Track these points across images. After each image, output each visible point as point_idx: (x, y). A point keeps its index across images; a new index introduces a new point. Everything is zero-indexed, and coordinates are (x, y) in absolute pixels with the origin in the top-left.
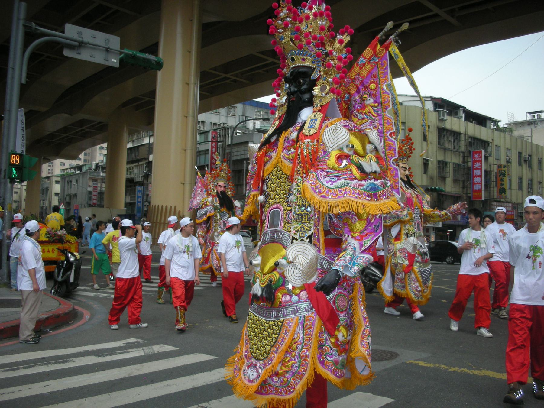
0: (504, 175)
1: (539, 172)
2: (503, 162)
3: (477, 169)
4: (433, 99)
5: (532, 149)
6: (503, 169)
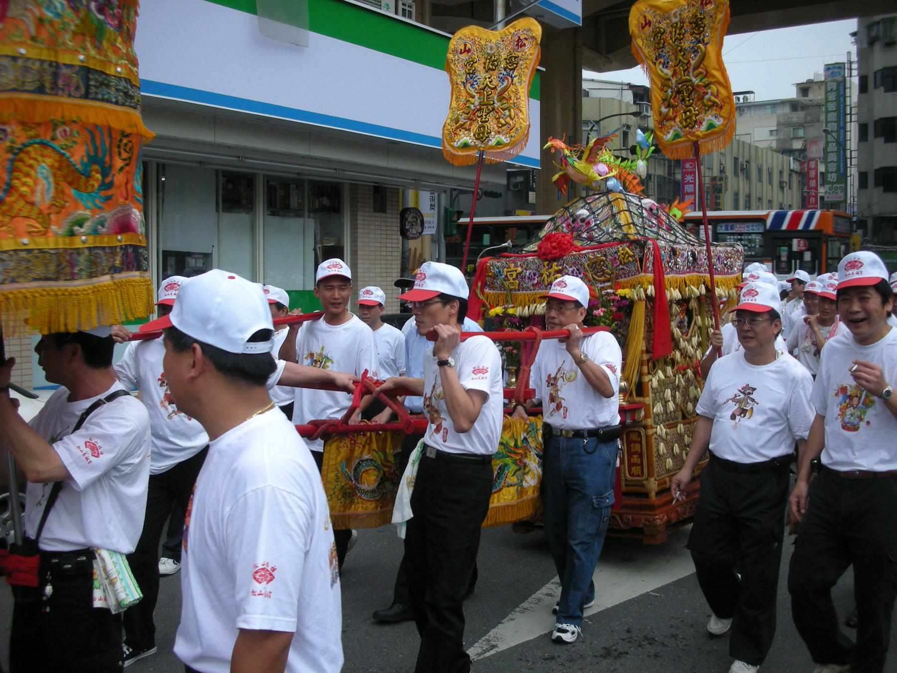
0: (720, 191)
1: (759, 184)
2: (716, 173)
3: (688, 183)
4: (631, 87)
5: (750, 152)
6: (719, 183)
